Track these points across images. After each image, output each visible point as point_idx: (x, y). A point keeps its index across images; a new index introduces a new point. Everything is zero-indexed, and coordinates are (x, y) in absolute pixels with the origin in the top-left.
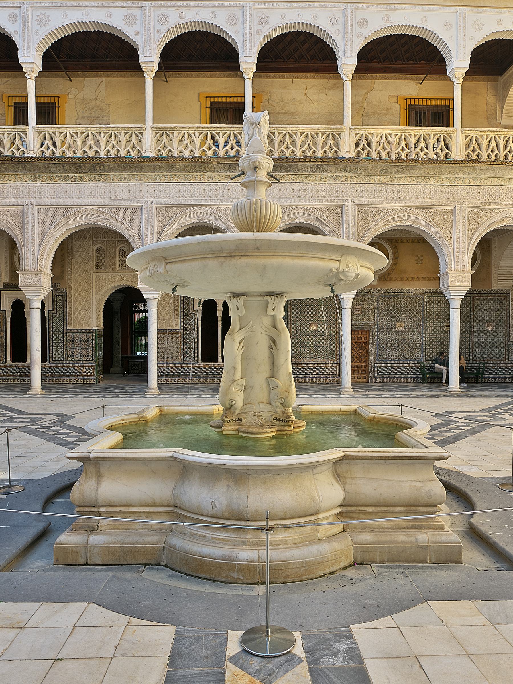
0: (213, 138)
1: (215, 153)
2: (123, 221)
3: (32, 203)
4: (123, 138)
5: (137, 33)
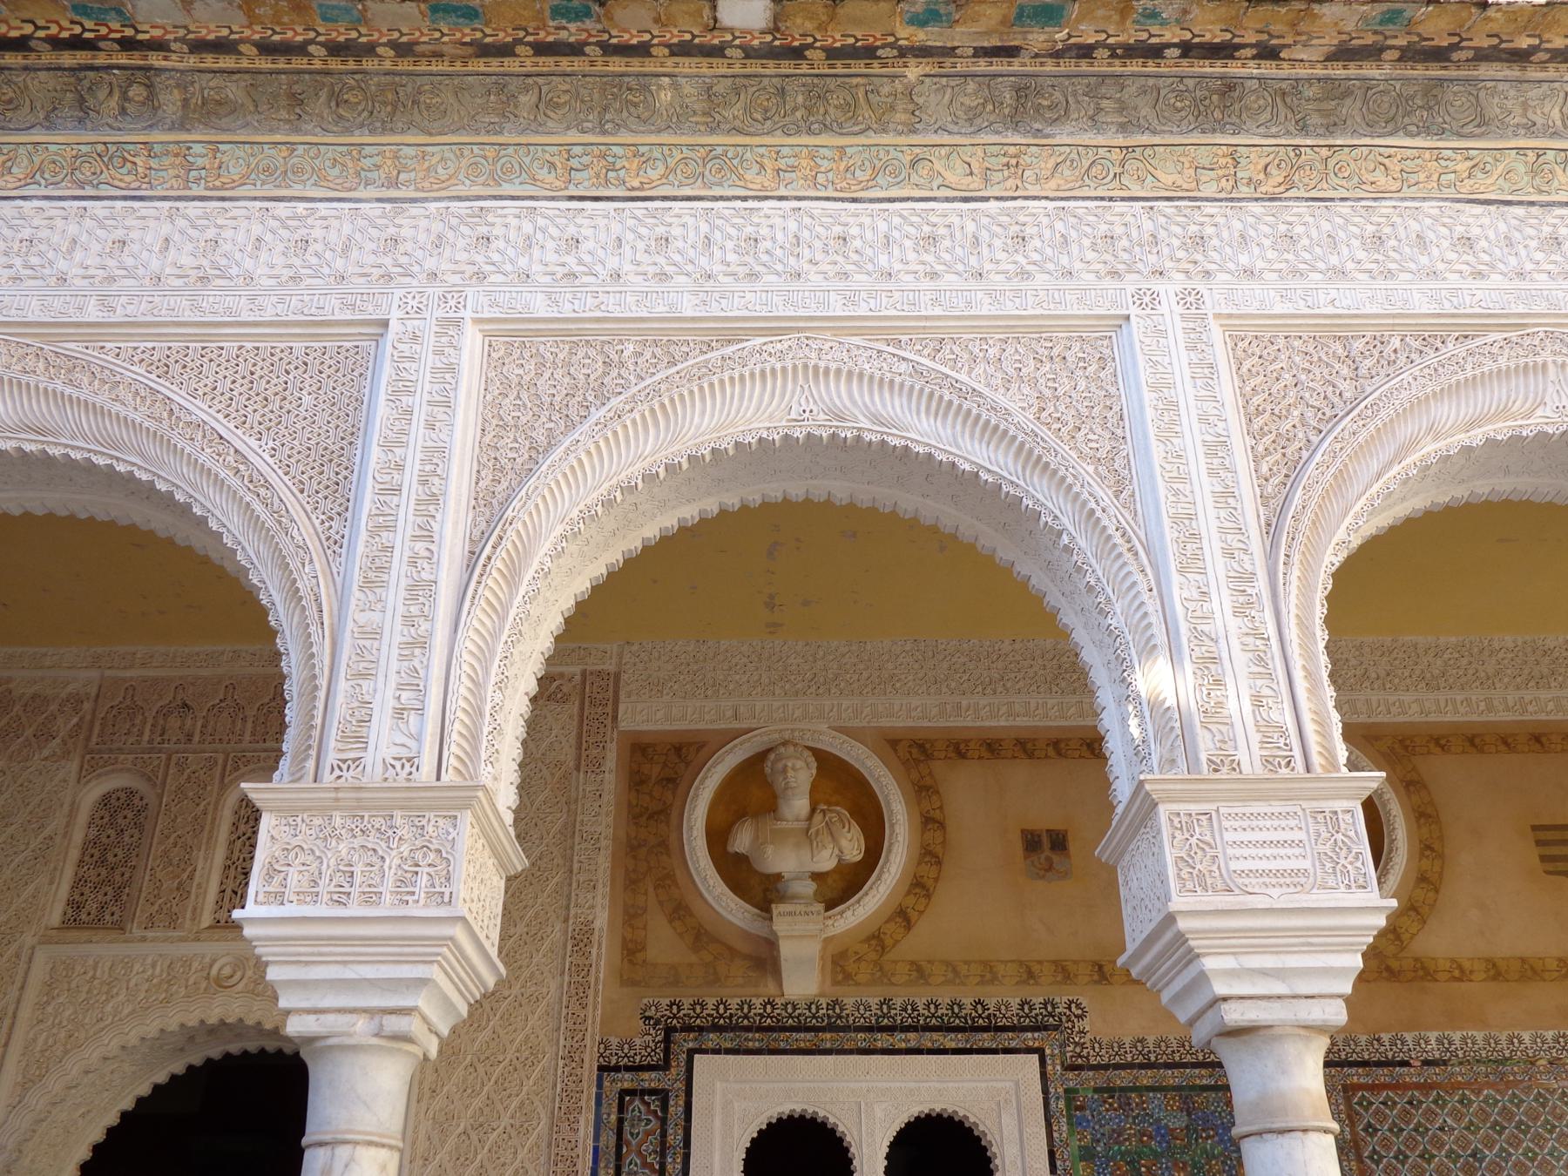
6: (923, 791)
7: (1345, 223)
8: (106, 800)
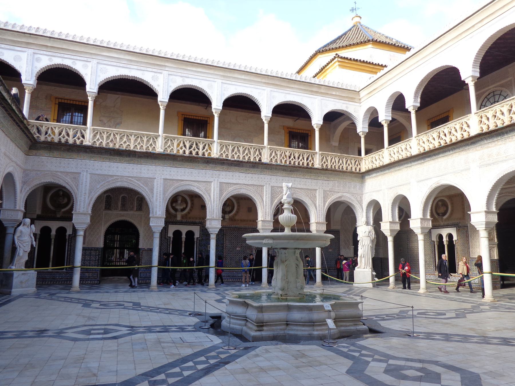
0: (197, 144)
1: (197, 153)
2: (143, 186)
3: (87, 171)
4: (145, 139)
5: (158, 85)
6: (192, 201)
7: (231, 174)
8: (107, 196)
